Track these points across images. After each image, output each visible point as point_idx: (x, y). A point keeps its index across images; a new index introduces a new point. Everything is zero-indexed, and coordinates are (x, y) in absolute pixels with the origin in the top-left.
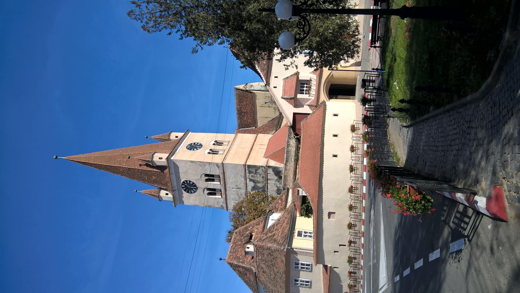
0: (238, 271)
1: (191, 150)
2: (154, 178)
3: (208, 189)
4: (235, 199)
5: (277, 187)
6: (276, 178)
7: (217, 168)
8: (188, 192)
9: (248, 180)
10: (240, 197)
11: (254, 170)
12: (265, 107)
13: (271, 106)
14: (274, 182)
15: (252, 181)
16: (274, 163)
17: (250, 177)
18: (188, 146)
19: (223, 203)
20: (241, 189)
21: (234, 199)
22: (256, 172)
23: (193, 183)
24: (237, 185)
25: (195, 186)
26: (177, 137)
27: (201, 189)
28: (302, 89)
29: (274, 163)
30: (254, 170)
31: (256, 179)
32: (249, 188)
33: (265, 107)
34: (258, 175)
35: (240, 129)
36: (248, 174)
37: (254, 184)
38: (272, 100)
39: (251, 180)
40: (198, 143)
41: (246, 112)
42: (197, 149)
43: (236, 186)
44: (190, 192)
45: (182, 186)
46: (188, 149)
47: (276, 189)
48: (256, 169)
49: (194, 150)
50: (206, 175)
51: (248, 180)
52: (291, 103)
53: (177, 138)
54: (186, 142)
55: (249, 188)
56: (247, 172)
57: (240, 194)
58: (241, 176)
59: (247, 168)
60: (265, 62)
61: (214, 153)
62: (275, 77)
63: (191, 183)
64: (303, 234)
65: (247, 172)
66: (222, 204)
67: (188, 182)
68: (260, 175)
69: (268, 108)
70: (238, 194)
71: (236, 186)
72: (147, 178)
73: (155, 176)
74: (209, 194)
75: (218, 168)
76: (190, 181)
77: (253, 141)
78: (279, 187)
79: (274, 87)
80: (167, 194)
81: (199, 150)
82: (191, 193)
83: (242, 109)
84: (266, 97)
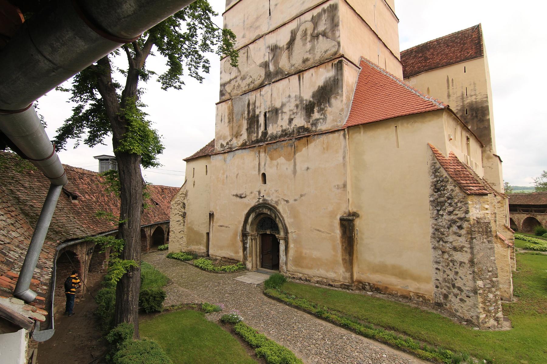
4: (246, 19)
5: (283, 105)
6: (307, 96)
9: (293, 26)
10: (251, 27)
11: (323, 29)
12: (448, 88)
13: (451, 98)
14: (293, 95)
15: (292, 36)
16: (350, 83)
20: (270, 19)
21: (246, 17)
24: (278, 5)
29: (350, 83)
30: (321, 28)
32: (271, 40)
33: (448, 88)
34: (309, 46)
36: (308, 16)
37: (283, 46)
38: (467, 97)
41: (426, 59)
43: (276, 5)
47: (278, 105)
48: (328, 31)
51: (293, 26)
55: (271, 40)
56: (315, 12)
57: (257, 24)
65: (315, 12)
68: (312, 49)
69: (446, 95)
70: (258, 18)
71: (276, 5)
78: (282, 112)
83: (432, 50)
84: (474, 84)
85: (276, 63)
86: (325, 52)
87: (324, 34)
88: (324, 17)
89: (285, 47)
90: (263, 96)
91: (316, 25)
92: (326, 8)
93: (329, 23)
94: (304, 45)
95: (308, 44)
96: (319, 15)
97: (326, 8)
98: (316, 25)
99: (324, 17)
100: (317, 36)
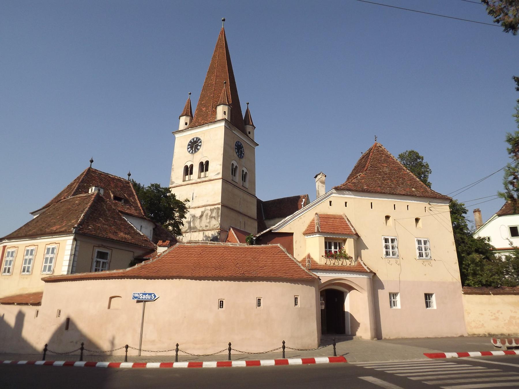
0: (74, 183)
1: (236, 145)
2: (204, 109)
3: (192, 166)
7: (216, 173)
8: (189, 145)
9: (203, 209)
15: (202, 214)
17: (206, 212)
18: (240, 143)
19: (176, 184)
22: (212, 217)
23: (198, 149)
24: (197, 197)
25: (195, 152)
26: (249, 133)
27: (192, 158)
28: (333, 244)
31: (204, 217)
34: (208, 220)
35: (261, 204)
39: (203, 213)
40: (244, 154)
42: (237, 153)
43: (196, 197)
44: (188, 147)
45: (195, 138)
46: (237, 143)
48: (216, 217)
49: (236, 149)
50: (207, 162)
51: (203, 209)
52: (309, 228)
53: (248, 133)
54: (245, 143)
56: (212, 207)
58: (208, 201)
59: (216, 206)
60: (366, 187)
61: (233, 171)
62: (346, 203)
63: (199, 147)
64: (102, 261)
65: (212, 207)
66: (176, 182)
67: (199, 144)
68: (209, 222)
71: (196, 197)
72: (204, 103)
73: (206, 110)
74: (186, 168)
75: (216, 175)
76: (200, 146)
77: (249, 215)
79: (330, 202)
80: (186, 124)
81: (236, 155)
82: (188, 148)
85: (194, 223)
86: (214, 225)
87: (214, 218)
88: (215, 211)
89: (199, 217)
90: (186, 237)
91: (212, 213)
92: (216, 207)
93: (216, 214)
94: (207, 219)
95: (208, 219)
96: (213, 209)
97: (216, 207)
98: (212, 213)
99: (215, 211)
100: (212, 217)
